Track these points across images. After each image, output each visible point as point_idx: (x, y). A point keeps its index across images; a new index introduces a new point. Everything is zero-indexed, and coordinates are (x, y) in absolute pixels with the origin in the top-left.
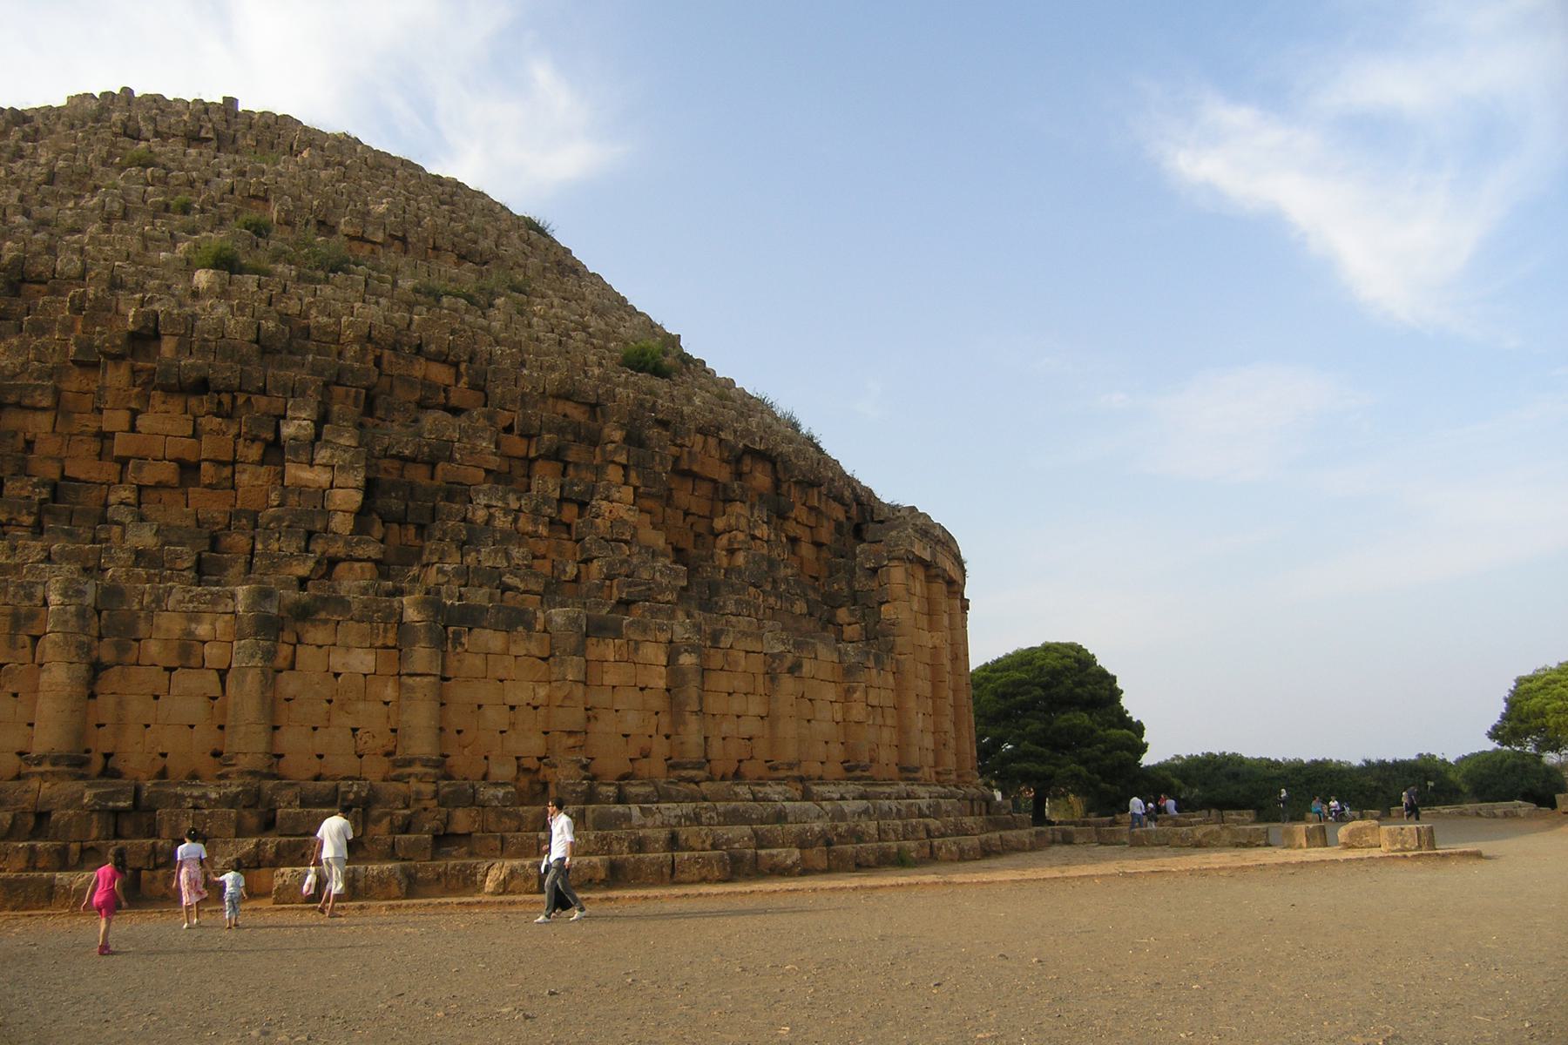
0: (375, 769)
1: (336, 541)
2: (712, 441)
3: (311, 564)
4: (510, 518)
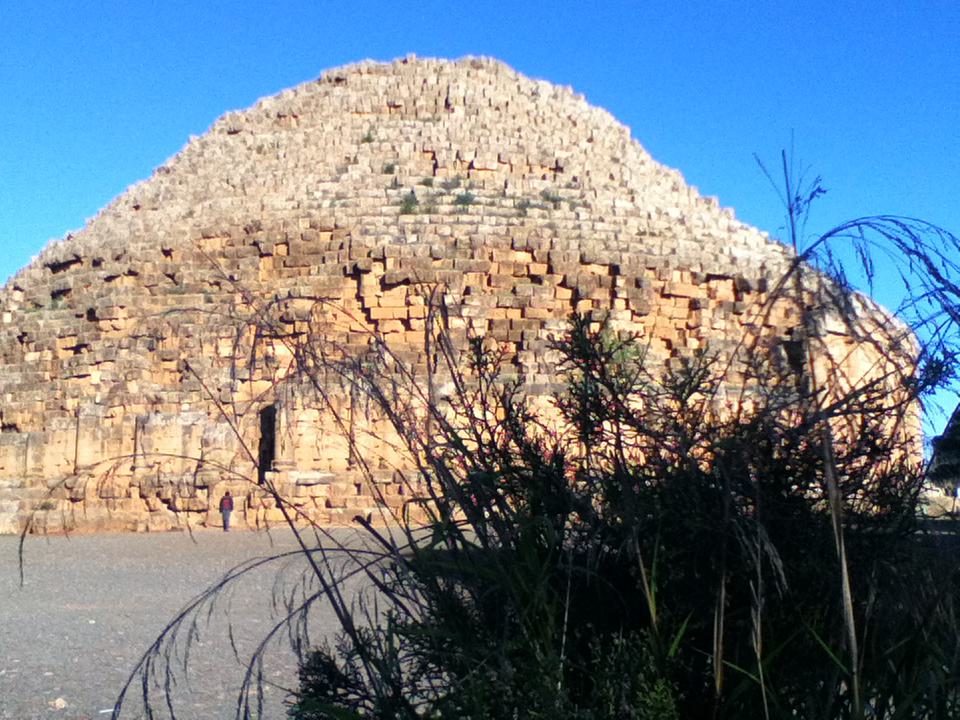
2: (686, 274)
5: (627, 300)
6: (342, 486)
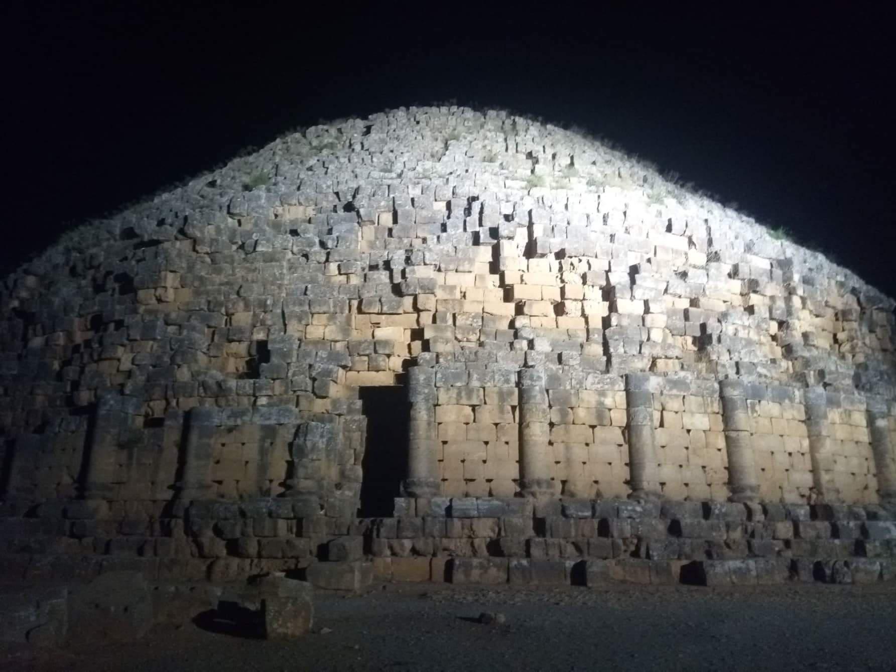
0: (721, 494)
1: (655, 346)
3: (646, 360)
4: (746, 331)
5: (803, 300)
6: (516, 520)
